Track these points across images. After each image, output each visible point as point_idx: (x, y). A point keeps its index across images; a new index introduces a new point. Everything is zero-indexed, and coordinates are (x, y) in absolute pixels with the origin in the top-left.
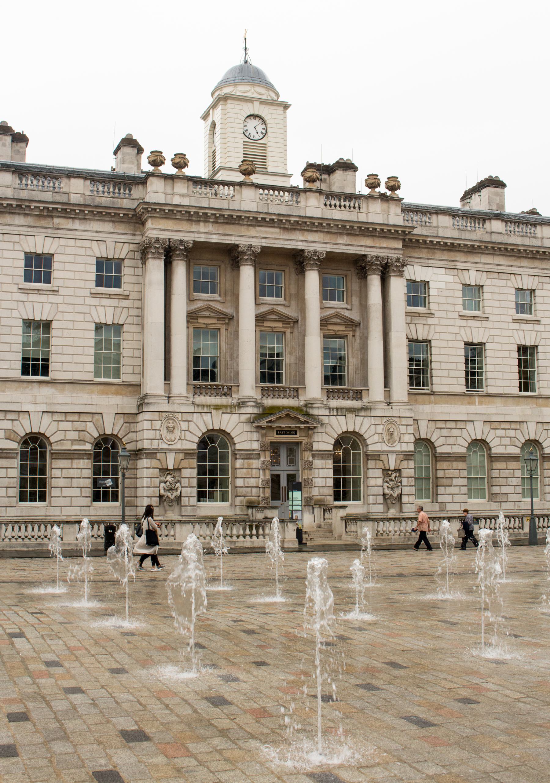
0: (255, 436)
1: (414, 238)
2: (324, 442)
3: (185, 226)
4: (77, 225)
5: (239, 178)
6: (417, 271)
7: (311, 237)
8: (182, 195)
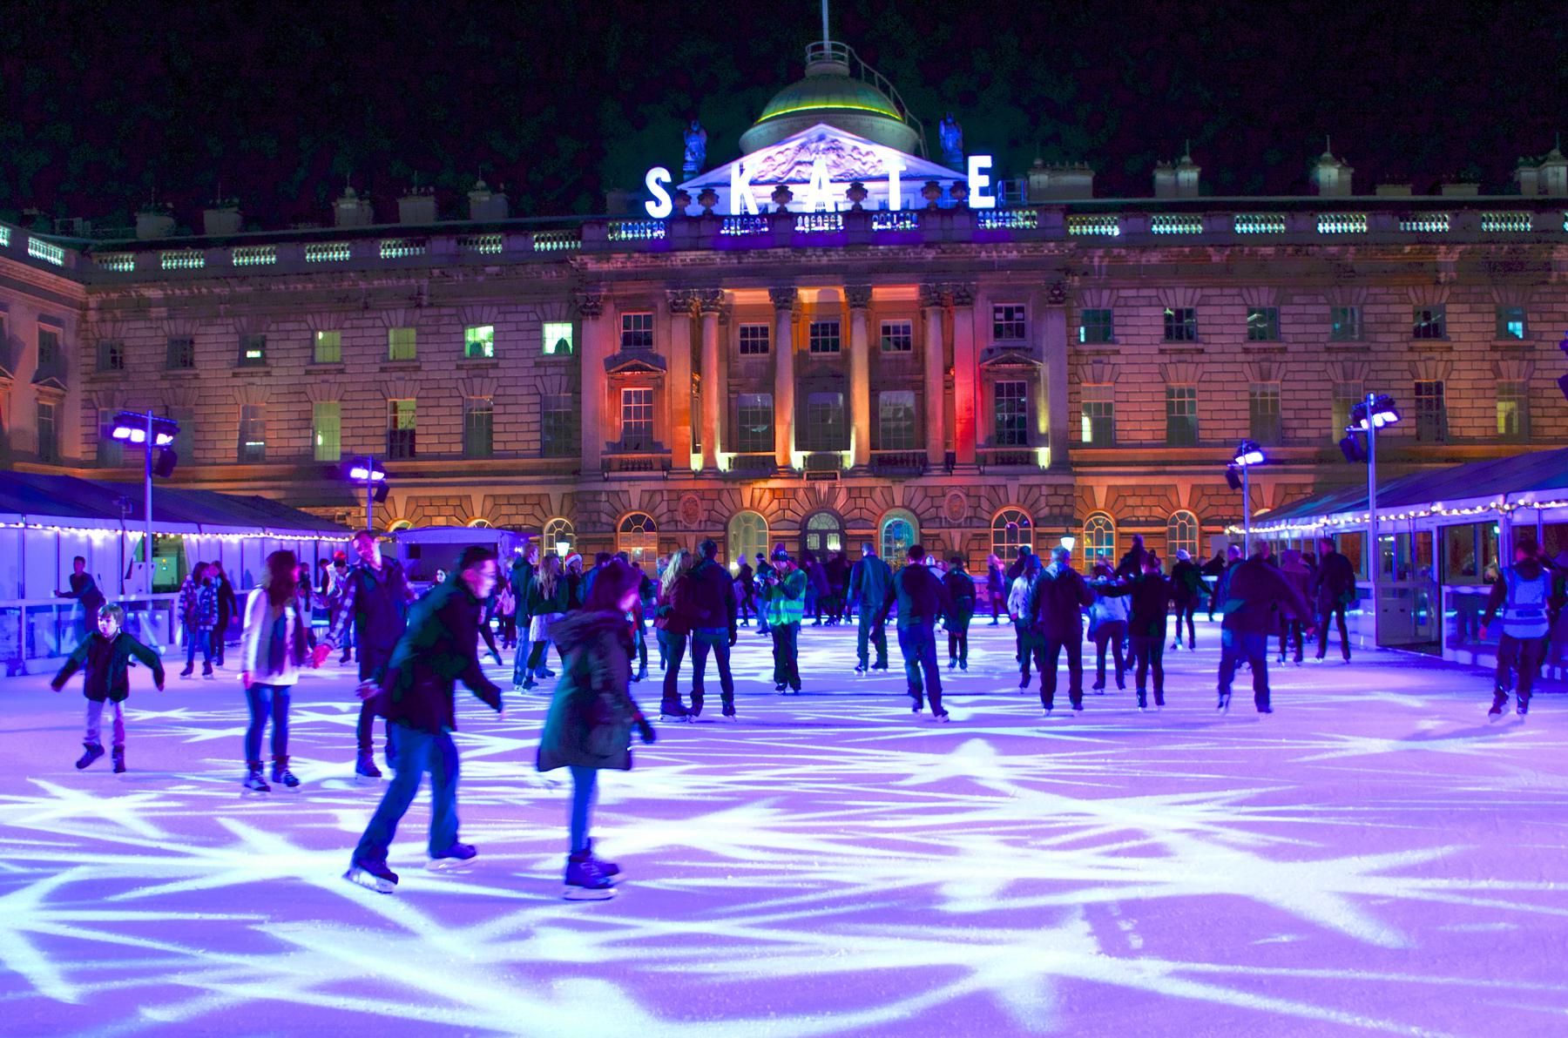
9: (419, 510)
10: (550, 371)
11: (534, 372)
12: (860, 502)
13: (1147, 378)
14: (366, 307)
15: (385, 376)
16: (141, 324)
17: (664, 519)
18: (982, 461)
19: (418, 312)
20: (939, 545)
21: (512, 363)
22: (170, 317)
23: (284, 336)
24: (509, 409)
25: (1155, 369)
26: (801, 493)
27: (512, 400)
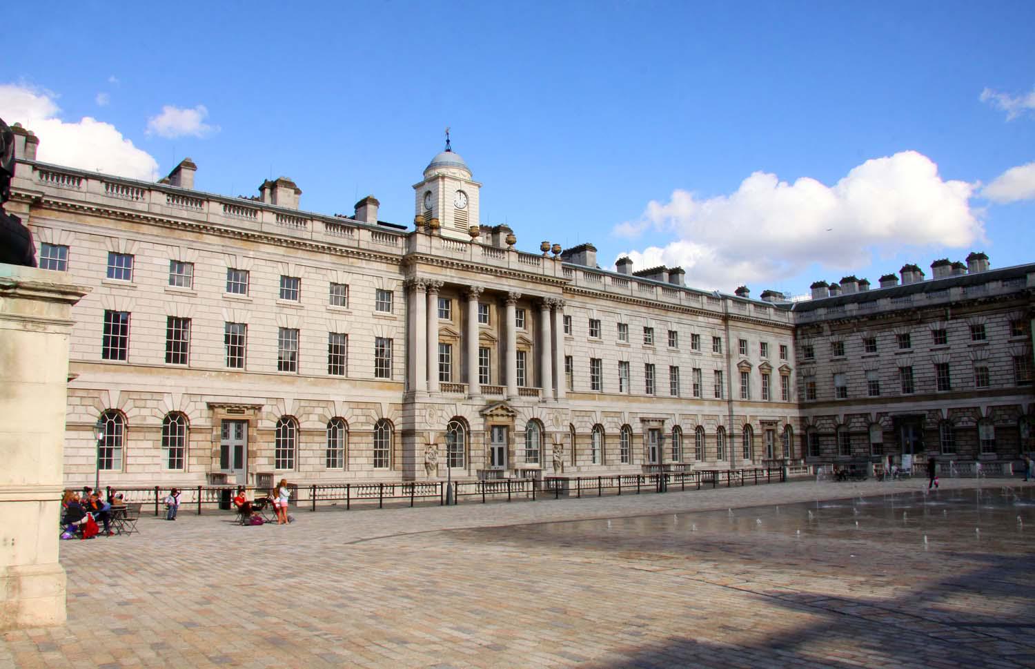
0: (482, 420)
1: (569, 287)
2: (520, 425)
3: (438, 270)
4: (364, 264)
5: (469, 238)
6: (567, 311)
7: (512, 282)
8: (437, 249)
9: (955, 414)
10: (1016, 344)
11: (1008, 345)
14: (920, 322)
15: (934, 353)
16: (820, 338)
19: (946, 322)
22: (832, 335)
23: (883, 338)
24: (997, 364)
27: (997, 360)
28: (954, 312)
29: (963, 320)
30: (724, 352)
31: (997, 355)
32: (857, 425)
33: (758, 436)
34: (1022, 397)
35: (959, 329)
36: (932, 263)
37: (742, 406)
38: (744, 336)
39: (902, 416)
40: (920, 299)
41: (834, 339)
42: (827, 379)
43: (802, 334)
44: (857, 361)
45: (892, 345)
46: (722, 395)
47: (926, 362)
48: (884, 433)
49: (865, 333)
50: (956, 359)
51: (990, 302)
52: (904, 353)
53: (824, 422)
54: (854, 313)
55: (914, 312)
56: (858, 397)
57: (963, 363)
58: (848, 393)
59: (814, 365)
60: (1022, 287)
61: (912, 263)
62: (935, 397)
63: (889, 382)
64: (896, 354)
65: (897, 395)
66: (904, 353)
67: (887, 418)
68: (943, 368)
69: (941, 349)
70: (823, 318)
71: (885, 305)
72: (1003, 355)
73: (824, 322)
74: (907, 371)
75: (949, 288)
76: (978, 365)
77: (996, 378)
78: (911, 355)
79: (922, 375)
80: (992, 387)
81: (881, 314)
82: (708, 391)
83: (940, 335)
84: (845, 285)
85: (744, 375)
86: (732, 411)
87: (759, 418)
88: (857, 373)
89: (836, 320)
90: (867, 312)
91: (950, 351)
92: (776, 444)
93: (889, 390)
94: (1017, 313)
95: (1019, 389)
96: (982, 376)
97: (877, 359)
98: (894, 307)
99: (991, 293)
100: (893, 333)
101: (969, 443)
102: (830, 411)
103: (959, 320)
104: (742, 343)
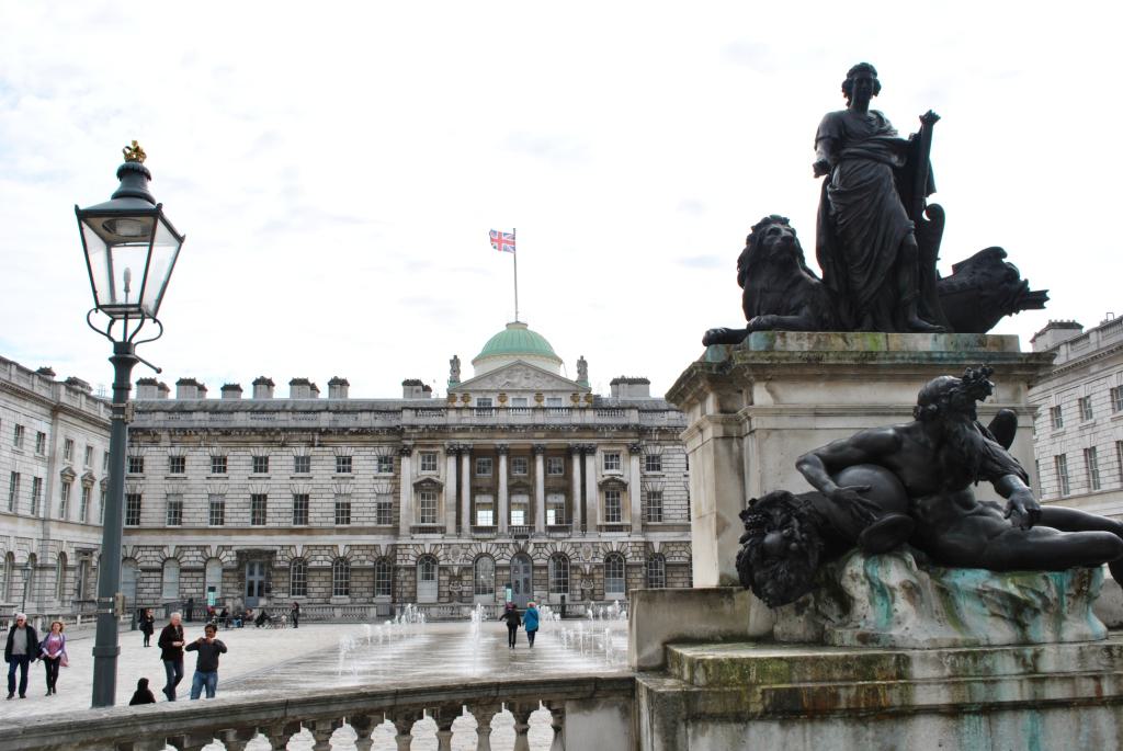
10: (382, 481)
12: (540, 550)
13: (679, 488)
14: (283, 445)
15: (293, 482)
16: (155, 449)
17: (442, 558)
18: (600, 528)
20: (579, 571)
21: (361, 476)
24: (360, 500)
25: (682, 484)
26: (511, 547)
28: (323, 439)
29: (331, 449)
30: (46, 453)
31: (360, 491)
32: (191, 559)
33: (73, 569)
34: (381, 537)
35: (325, 458)
36: (290, 380)
37: (59, 528)
38: (73, 435)
39: (249, 550)
40: (283, 420)
41: (176, 452)
42: (158, 501)
43: (131, 441)
44: (201, 482)
45: (244, 468)
46: (38, 512)
47: (283, 491)
48: (224, 570)
49: (214, 449)
50: (319, 491)
51: (361, 433)
52: (260, 478)
53: (147, 553)
54: (203, 424)
55: (278, 433)
56: (196, 525)
57: (324, 496)
58: (183, 520)
59: (142, 482)
60: (394, 423)
61: (268, 377)
62: (291, 531)
63: (236, 510)
64: (250, 478)
65: (245, 526)
66: (260, 478)
67: (230, 553)
68: (302, 502)
69: (302, 478)
70: (162, 424)
71: (241, 420)
72: (368, 491)
73: (164, 429)
74: (259, 501)
75: (319, 411)
76: (340, 500)
77: (357, 515)
78: (268, 481)
79: (278, 506)
80: (352, 525)
81: (239, 429)
82: (24, 506)
83: (344, 463)
84: (182, 387)
85: (66, 486)
86: (48, 534)
87: (75, 545)
88: (199, 496)
89: (181, 429)
90: (219, 425)
91: (311, 482)
92: (89, 580)
93: (237, 520)
94: (386, 449)
95: (380, 529)
96: (343, 512)
97: (226, 482)
98: (253, 424)
99: (362, 425)
100: (248, 453)
101: (322, 585)
102: (158, 540)
103: (327, 449)
104: (69, 443)
